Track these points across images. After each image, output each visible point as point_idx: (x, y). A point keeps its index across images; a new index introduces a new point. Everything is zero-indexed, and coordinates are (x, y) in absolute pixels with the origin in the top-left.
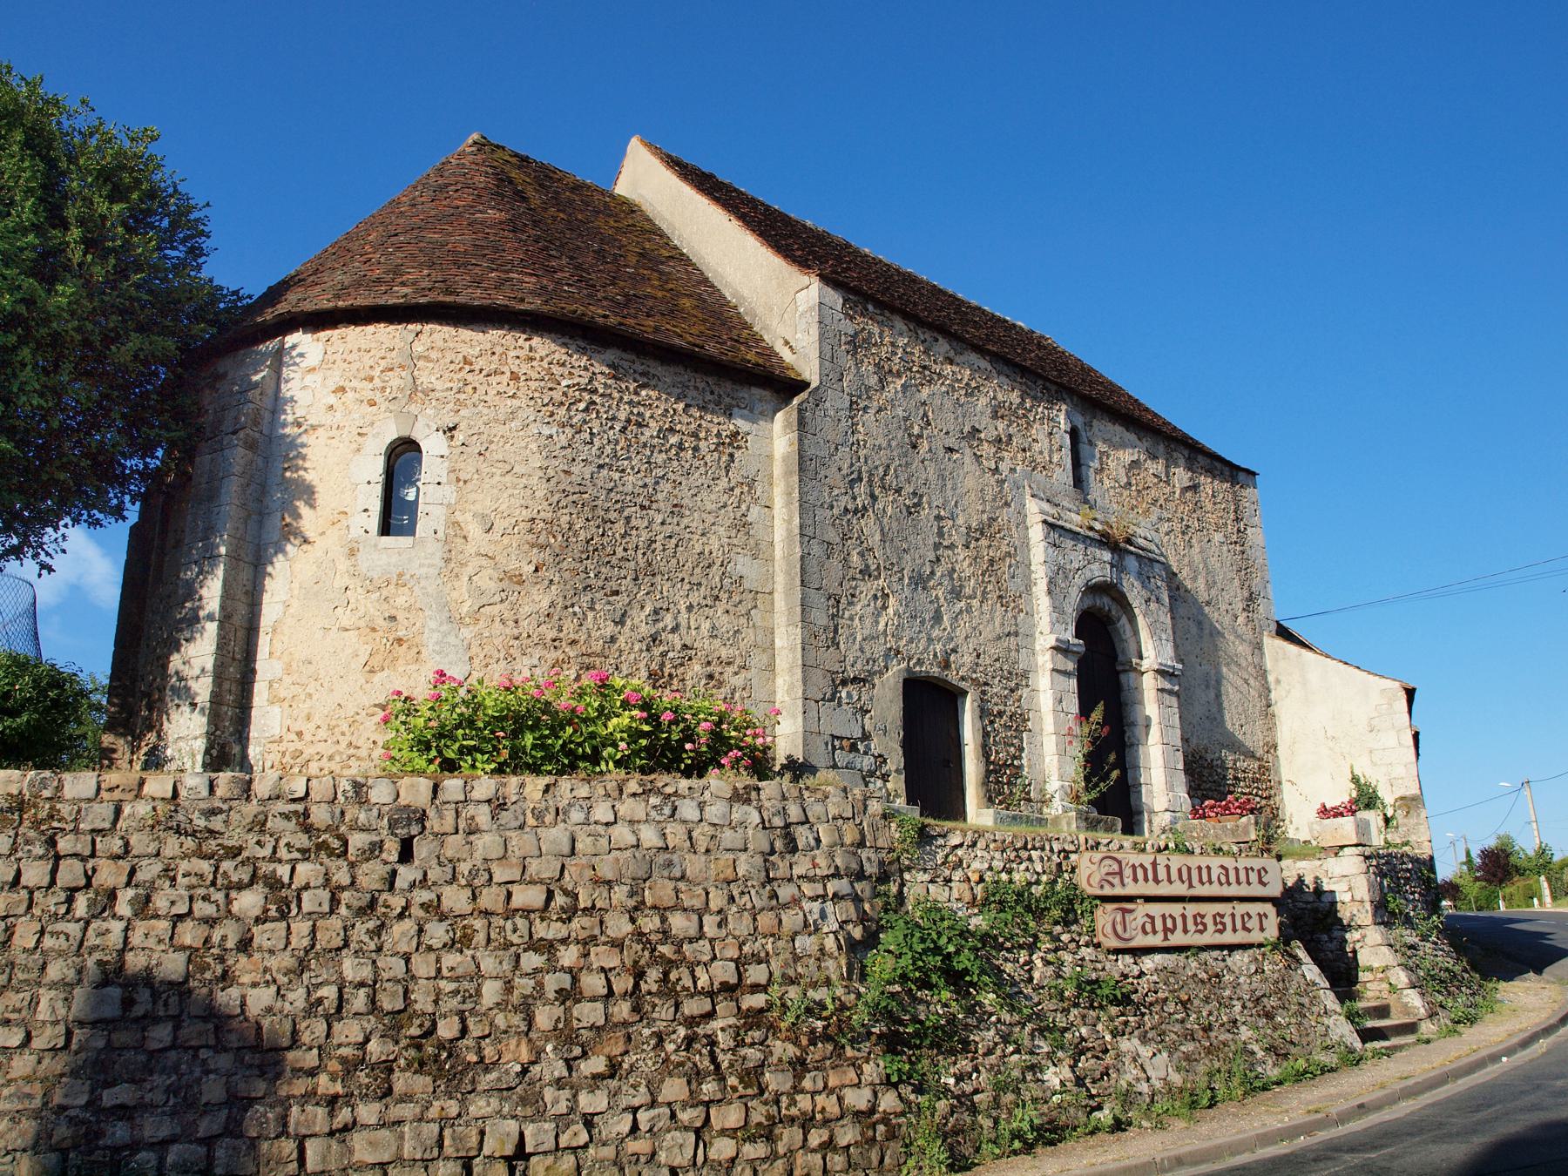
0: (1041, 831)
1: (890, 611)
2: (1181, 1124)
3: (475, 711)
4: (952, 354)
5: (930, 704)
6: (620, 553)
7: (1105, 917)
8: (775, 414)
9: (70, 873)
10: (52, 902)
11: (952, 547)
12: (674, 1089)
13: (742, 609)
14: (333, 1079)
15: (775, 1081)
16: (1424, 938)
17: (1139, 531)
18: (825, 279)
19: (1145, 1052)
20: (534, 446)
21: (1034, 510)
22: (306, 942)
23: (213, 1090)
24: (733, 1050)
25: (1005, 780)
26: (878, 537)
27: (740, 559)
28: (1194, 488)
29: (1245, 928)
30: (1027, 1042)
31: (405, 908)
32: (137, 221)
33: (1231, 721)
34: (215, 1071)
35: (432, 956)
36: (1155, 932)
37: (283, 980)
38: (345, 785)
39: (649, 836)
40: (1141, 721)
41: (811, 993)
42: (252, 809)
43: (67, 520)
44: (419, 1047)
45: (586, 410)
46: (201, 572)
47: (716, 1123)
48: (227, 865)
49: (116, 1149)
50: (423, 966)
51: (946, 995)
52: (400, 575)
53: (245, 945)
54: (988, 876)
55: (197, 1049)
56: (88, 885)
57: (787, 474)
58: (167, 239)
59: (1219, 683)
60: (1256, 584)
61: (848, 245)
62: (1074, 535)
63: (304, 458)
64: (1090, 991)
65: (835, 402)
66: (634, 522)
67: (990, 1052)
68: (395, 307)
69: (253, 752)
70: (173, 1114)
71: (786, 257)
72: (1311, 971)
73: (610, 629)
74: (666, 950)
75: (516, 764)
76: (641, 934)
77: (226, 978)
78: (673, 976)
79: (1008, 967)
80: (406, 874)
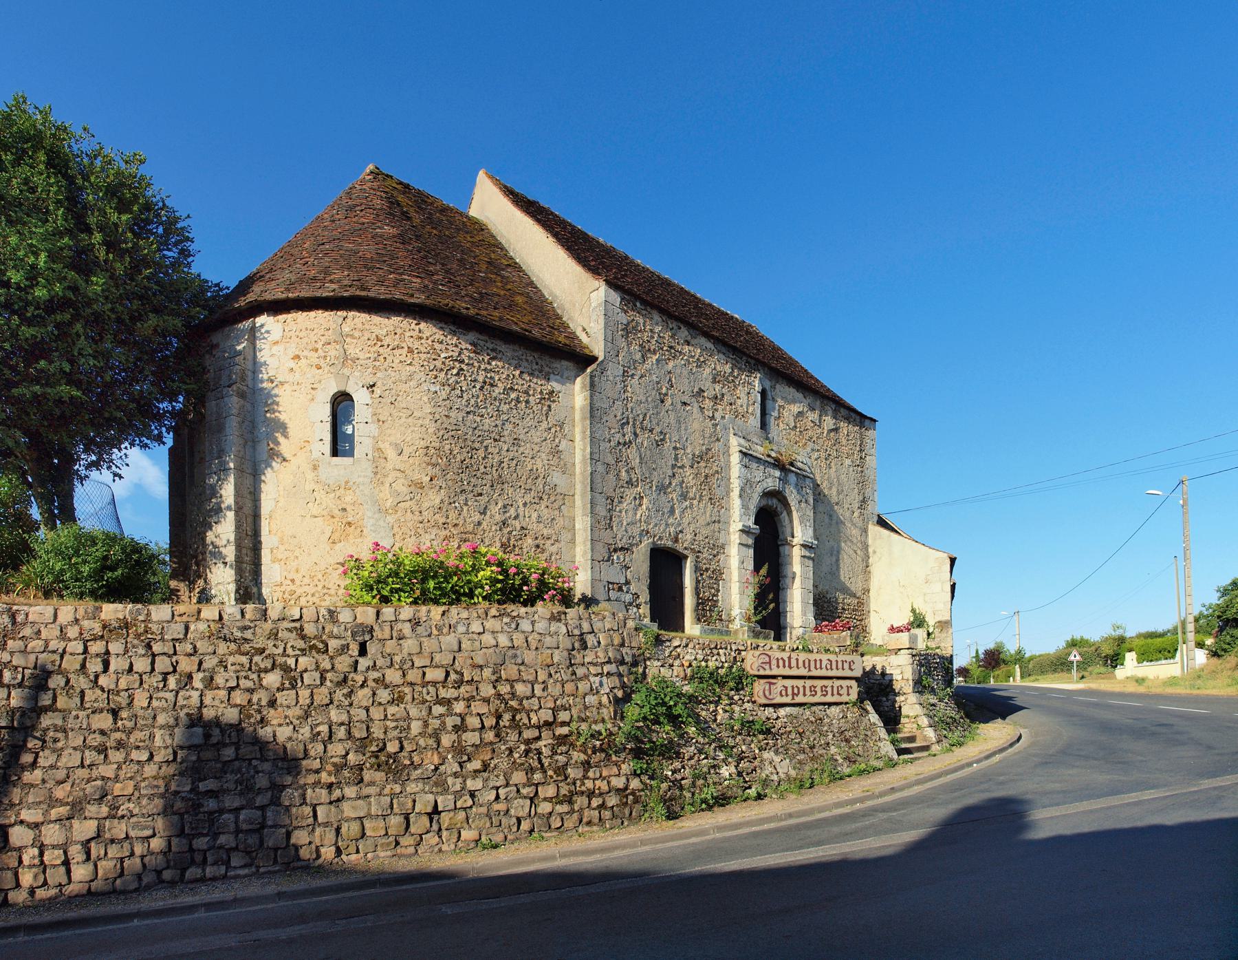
0: (726, 638)
1: (644, 507)
2: (793, 796)
3: (399, 566)
4: (689, 338)
5: (666, 563)
6: (482, 469)
7: (759, 686)
8: (576, 377)
9: (163, 664)
10: (155, 680)
11: (682, 467)
12: (519, 777)
13: (556, 505)
14: (330, 774)
15: (572, 773)
16: (941, 700)
17: (799, 458)
18: (610, 284)
19: (777, 759)
20: (425, 399)
21: (735, 443)
22: (308, 701)
23: (262, 781)
24: (551, 757)
25: (707, 609)
27: (555, 474)
28: (836, 430)
30: (712, 753)
31: (365, 682)
32: (140, 228)
33: (844, 575)
34: (262, 771)
35: (382, 708)
37: (296, 722)
38: (323, 612)
39: (503, 640)
40: (790, 575)
41: (593, 726)
42: (268, 626)
43: (126, 444)
44: (377, 757)
45: (458, 374)
46: (219, 479)
47: (541, 794)
48: (257, 659)
49: (211, 813)
50: (376, 713)
51: (668, 728)
52: (347, 482)
53: (272, 703)
54: (694, 664)
55: (250, 760)
56: (175, 671)
57: (583, 419)
58: (164, 243)
59: (838, 552)
60: (868, 492)
61: (627, 257)
62: (758, 460)
63: (277, 404)
64: (748, 727)
65: (614, 371)
66: (490, 450)
67: (691, 758)
68: (327, 298)
69: (265, 591)
70: (241, 794)
71: (584, 266)
72: (874, 717)
73: (477, 517)
74: (513, 703)
75: (424, 598)
76: (500, 695)
77: (263, 721)
78: (518, 718)
79: (704, 713)
80: (364, 663)
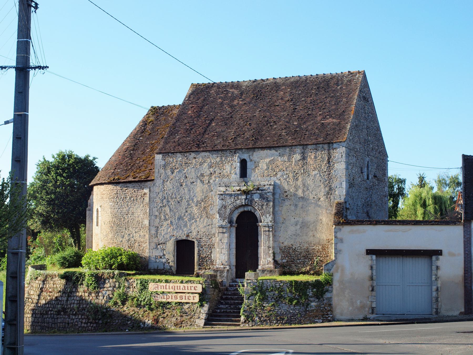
13: (145, 231)
26: (169, 211)
27: (145, 221)
29: (188, 299)
36: (164, 298)
73: (121, 239)
